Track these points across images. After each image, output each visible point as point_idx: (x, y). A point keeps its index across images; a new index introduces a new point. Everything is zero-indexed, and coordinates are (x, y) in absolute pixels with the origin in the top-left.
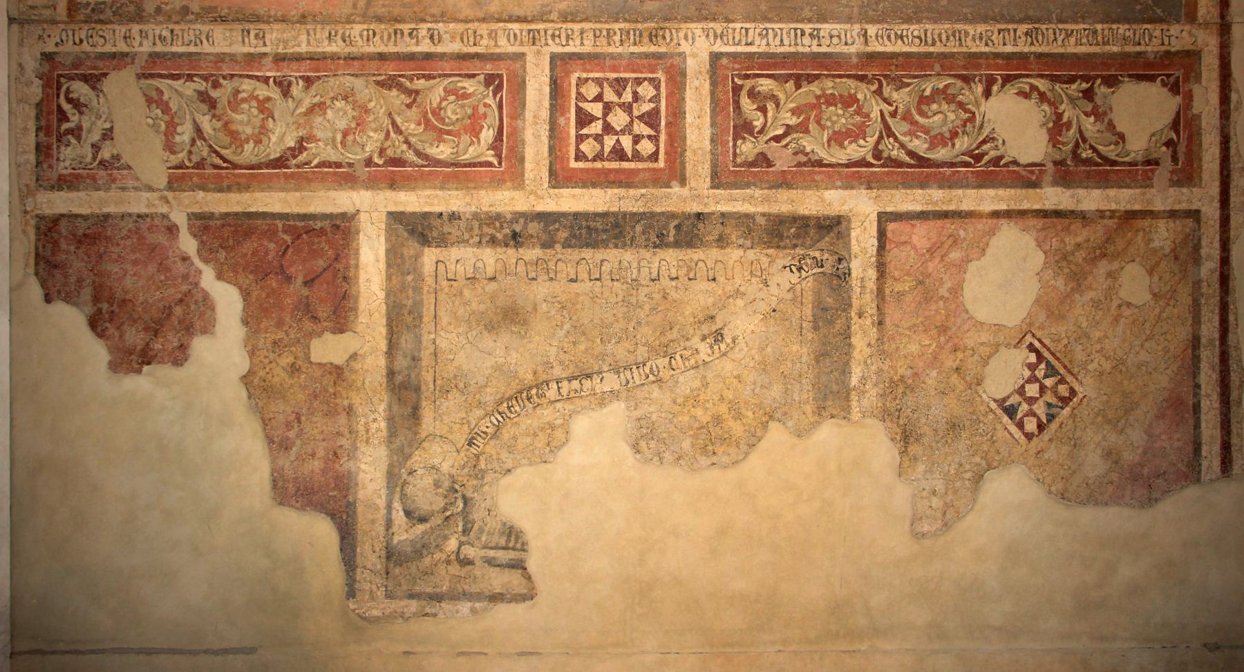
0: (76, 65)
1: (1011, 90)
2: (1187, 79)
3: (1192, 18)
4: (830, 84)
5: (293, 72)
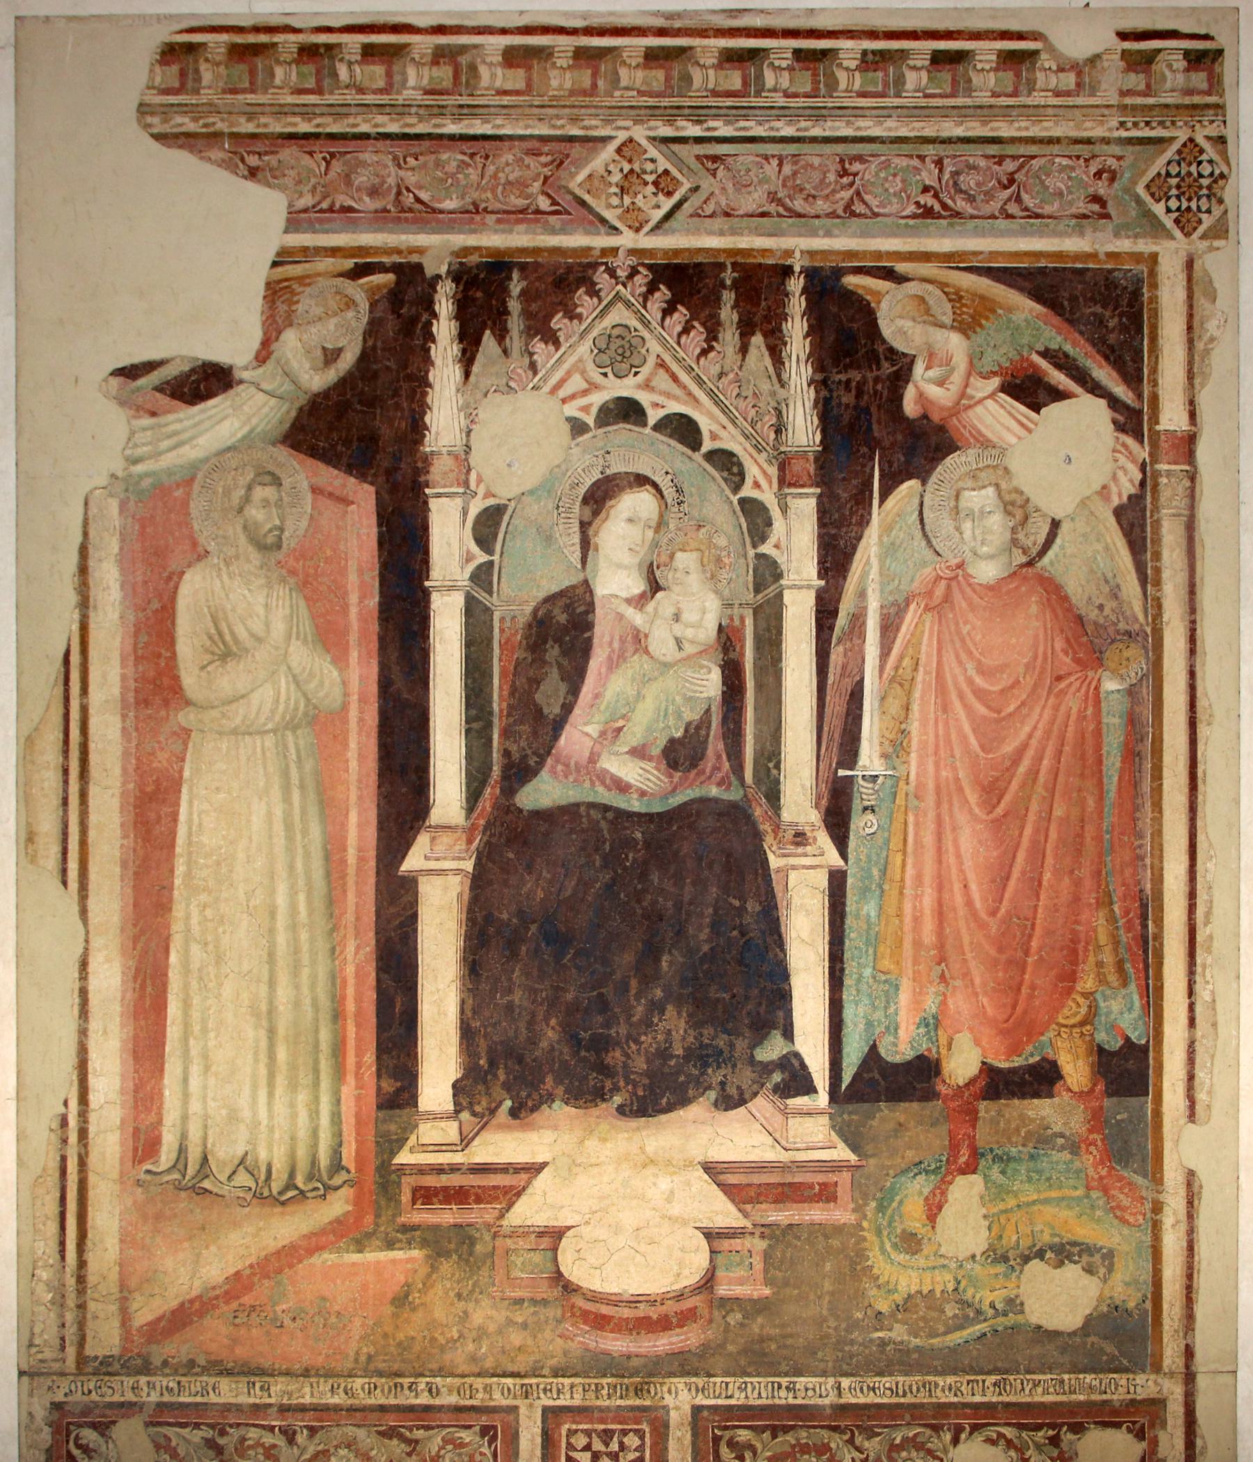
0: (84, 1413)
1: (978, 1438)
2: (1152, 1425)
3: (1157, 1368)
4: (805, 1434)
5: (298, 1422)
